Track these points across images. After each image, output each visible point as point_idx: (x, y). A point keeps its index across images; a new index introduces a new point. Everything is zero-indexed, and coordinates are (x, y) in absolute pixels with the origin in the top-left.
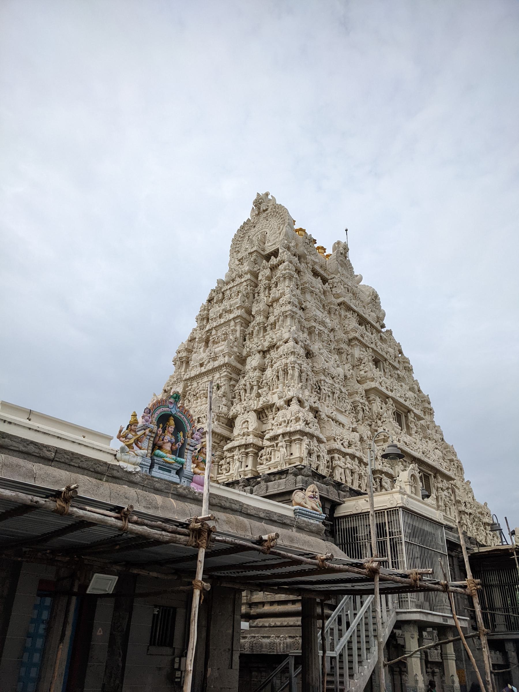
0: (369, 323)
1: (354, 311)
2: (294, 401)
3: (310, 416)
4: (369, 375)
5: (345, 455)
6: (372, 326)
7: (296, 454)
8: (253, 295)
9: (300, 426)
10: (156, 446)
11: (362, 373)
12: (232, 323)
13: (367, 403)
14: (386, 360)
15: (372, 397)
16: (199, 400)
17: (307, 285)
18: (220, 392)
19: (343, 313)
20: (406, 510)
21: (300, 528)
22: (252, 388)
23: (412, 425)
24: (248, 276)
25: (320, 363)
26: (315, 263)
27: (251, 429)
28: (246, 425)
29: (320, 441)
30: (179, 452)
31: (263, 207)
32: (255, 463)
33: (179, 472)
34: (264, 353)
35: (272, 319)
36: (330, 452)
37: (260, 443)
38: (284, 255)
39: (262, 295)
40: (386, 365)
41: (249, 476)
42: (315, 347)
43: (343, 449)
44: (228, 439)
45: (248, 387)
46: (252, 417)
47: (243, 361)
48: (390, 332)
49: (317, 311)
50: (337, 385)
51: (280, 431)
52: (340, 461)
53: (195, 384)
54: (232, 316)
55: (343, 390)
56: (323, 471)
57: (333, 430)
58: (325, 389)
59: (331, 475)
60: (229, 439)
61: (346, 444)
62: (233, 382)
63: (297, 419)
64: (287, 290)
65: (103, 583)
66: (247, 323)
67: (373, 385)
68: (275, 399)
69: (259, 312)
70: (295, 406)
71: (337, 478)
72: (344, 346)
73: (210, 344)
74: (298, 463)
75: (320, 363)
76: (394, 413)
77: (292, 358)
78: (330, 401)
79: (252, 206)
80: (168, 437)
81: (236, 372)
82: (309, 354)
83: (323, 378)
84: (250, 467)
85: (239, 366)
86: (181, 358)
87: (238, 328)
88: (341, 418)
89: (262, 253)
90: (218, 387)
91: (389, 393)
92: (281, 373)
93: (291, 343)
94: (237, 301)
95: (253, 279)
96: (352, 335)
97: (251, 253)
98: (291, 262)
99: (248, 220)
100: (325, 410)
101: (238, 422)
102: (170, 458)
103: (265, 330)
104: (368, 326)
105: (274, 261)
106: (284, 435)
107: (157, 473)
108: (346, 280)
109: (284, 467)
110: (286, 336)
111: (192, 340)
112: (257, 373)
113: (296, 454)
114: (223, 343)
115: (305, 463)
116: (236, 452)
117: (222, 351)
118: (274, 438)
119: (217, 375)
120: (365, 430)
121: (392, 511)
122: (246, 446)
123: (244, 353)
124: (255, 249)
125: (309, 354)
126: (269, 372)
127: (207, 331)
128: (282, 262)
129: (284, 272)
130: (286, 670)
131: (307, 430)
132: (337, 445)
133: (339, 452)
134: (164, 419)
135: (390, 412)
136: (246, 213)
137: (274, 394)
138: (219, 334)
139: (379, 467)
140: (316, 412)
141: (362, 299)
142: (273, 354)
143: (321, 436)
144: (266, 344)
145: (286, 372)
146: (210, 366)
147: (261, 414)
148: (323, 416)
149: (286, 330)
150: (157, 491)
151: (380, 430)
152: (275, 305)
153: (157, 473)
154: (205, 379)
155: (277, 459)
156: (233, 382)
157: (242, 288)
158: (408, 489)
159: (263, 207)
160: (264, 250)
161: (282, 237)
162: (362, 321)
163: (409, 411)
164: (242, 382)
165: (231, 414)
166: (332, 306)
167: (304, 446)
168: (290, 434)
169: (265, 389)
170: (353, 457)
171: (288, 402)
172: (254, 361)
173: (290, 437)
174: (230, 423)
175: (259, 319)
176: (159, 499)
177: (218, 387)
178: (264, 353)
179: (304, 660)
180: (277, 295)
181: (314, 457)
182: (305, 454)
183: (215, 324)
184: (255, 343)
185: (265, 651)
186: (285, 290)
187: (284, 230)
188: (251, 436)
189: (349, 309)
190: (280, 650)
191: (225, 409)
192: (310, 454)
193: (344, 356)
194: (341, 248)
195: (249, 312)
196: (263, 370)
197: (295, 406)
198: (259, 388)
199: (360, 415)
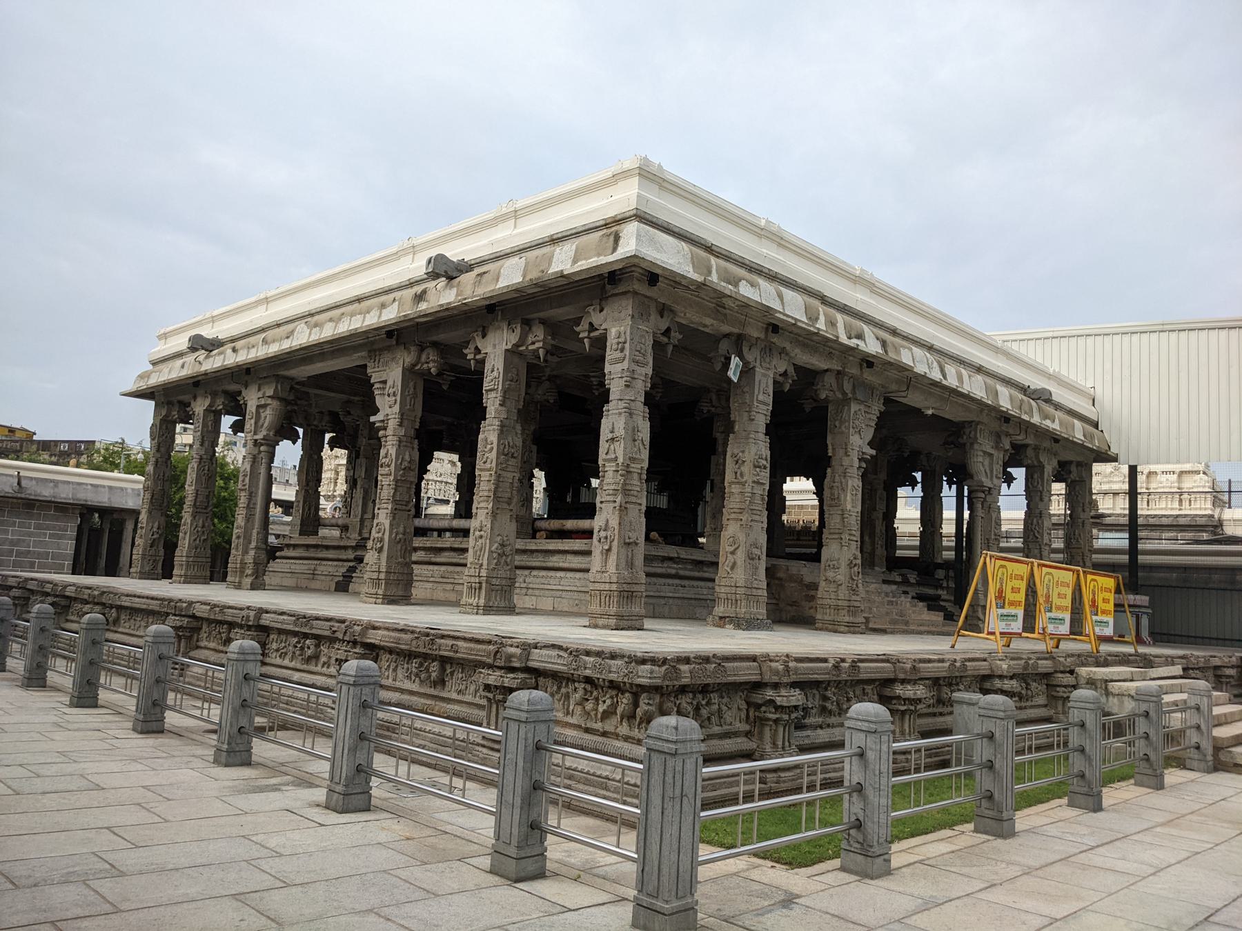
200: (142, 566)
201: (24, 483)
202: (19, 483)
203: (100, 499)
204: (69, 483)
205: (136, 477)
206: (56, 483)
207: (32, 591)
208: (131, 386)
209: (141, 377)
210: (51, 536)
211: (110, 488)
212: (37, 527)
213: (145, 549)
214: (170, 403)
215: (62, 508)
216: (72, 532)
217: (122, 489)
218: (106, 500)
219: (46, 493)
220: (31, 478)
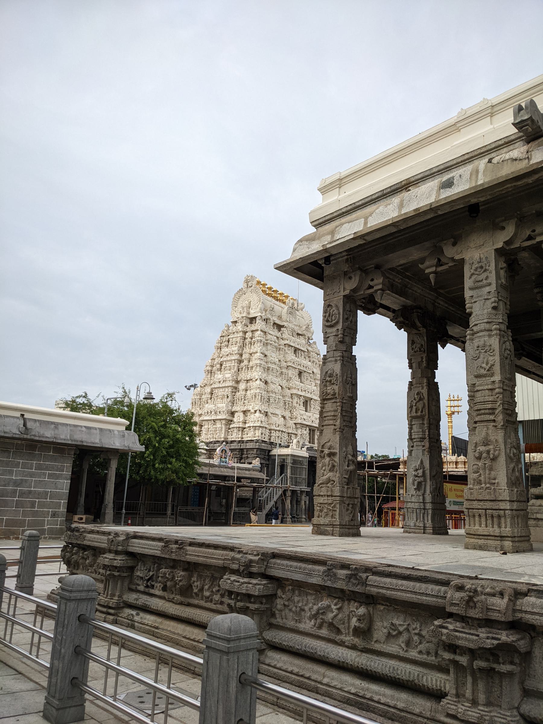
0: (299, 349)
1: (292, 346)
2: (258, 412)
3: (263, 418)
4: (294, 386)
5: (276, 430)
6: (301, 350)
7: (257, 435)
8: (243, 346)
9: (258, 424)
10: (221, 457)
11: (291, 384)
12: (233, 362)
13: (291, 400)
14: (305, 372)
15: (294, 396)
16: (219, 400)
17: (268, 342)
18: (229, 400)
19: (286, 348)
20: (292, 455)
21: (254, 470)
22: (242, 399)
23: (312, 406)
24: (241, 334)
25: (272, 387)
26: (274, 321)
27: (241, 420)
28: (239, 418)
29: (266, 428)
30: (225, 458)
31: (250, 284)
32: (242, 434)
33: (226, 462)
34: (247, 381)
35: (251, 364)
36: (270, 430)
37: (244, 426)
38: (259, 325)
39: (247, 346)
40: (305, 374)
41: (240, 439)
42: (269, 378)
43: (276, 429)
44: (231, 421)
45: (240, 398)
46: (241, 415)
47: (238, 382)
48: (315, 343)
49: (274, 355)
50: (277, 397)
51: (252, 425)
52: (273, 434)
53: (217, 391)
54: (233, 358)
55: (280, 397)
56: (266, 440)
57: (274, 419)
58: (272, 400)
59: (270, 439)
60: (231, 421)
61: (277, 425)
62: (233, 394)
63: (258, 421)
64: (259, 351)
65: (213, 488)
66: (240, 361)
67: (294, 391)
68: (250, 408)
69: (246, 359)
70: (257, 414)
71: (272, 441)
72: (284, 370)
73: (222, 370)
74: (257, 438)
75: (272, 387)
76: (304, 403)
77: (258, 391)
78: (273, 406)
79: (244, 280)
80: (224, 455)
81: (235, 389)
82: (266, 383)
83: (271, 395)
84: (240, 436)
85: (236, 385)
86: (208, 370)
87: (236, 364)
88: (278, 412)
89: (248, 316)
90: (228, 397)
91: (303, 394)
92: (253, 397)
93: (258, 382)
94: (235, 348)
95: (244, 336)
96: (289, 364)
97: (242, 317)
98: (261, 331)
99: (242, 288)
100: (270, 410)
101: (236, 415)
102: (224, 460)
103: (248, 369)
104: (300, 352)
105: (253, 327)
106: (253, 427)
107: (222, 464)
108: (290, 325)
109: (253, 439)
110: (257, 377)
111: (213, 359)
112: (244, 393)
113: (257, 435)
114: (229, 372)
115: (260, 438)
116: (235, 429)
117: (229, 378)
118: (250, 427)
119: (227, 390)
120: (287, 414)
121: (288, 455)
122: (239, 427)
123: (239, 380)
124: (244, 315)
125: (266, 383)
126: (248, 392)
127: (221, 362)
128: (257, 330)
129: (258, 338)
130: (249, 503)
131: (262, 425)
132: (273, 427)
133: (274, 430)
134: (223, 450)
135: (302, 404)
136: (241, 285)
137: (250, 405)
138: (227, 365)
139: (290, 432)
140: (266, 414)
141: (301, 326)
142: (251, 383)
143: (267, 426)
144: (248, 379)
145: (255, 396)
146: (224, 385)
147: (245, 412)
148: (269, 414)
149: (256, 374)
150: (222, 467)
151: (295, 414)
152: (253, 355)
153: (222, 464)
154: (221, 390)
155: (249, 436)
156: (233, 394)
157: (238, 339)
158: (294, 447)
159: (250, 284)
160: (249, 313)
161: (258, 310)
162: (296, 350)
163: (312, 399)
164: (237, 394)
165: (233, 410)
166: (281, 347)
167: (260, 432)
168: (255, 427)
169: (247, 401)
170: (279, 431)
171: (256, 411)
172: (242, 386)
173: (255, 427)
174: (233, 414)
175: (246, 362)
176: (222, 469)
177: (228, 397)
178: (247, 381)
179: (253, 501)
180: (254, 351)
181: (263, 435)
182: (260, 435)
183: (225, 359)
184: (243, 376)
185: (243, 497)
186: (257, 348)
187: (259, 306)
188: (241, 423)
189: (290, 346)
190: (248, 497)
191: (230, 408)
192: (262, 434)
193: (284, 376)
194: (290, 304)
195: (241, 355)
196: (246, 390)
197: (257, 414)
198: (245, 400)
199: (287, 408)
200: (341, 515)
201: (29, 425)
202: (25, 425)
203: (93, 440)
204: (67, 425)
205: (119, 420)
206: (57, 425)
207: (279, 582)
208: (287, 255)
209: (309, 239)
210: (50, 476)
211: (101, 430)
212: (39, 467)
213: (342, 491)
214: (365, 271)
215: (59, 448)
216: (67, 473)
217: (110, 430)
218: (97, 441)
219: (48, 434)
220: (35, 421)
